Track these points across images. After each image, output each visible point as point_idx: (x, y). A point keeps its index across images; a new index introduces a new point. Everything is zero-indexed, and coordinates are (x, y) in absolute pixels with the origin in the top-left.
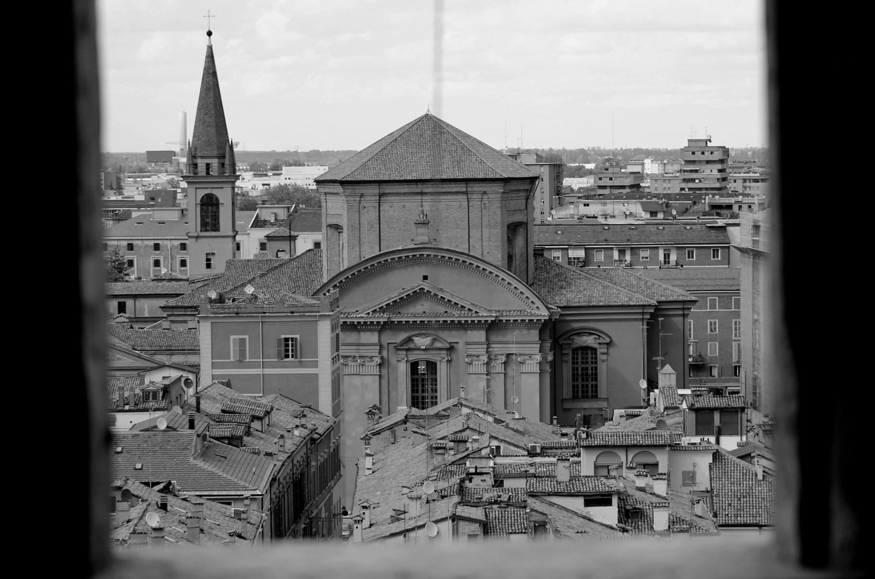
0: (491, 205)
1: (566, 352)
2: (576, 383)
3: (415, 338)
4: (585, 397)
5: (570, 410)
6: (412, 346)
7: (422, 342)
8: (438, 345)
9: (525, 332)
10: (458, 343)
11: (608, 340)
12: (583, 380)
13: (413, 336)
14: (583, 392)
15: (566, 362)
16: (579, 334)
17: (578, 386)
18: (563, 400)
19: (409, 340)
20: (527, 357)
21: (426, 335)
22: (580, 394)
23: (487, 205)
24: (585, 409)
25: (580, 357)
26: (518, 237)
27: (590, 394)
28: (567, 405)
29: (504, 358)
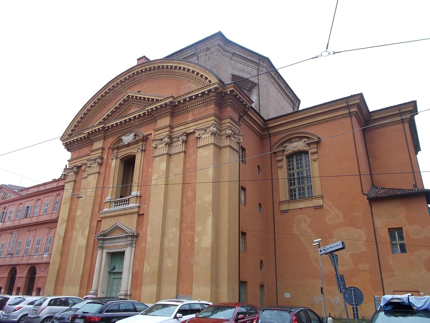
1: (280, 158)
2: (293, 187)
3: (123, 138)
4: (303, 198)
5: (287, 211)
6: (121, 144)
7: (127, 139)
8: (137, 138)
9: (203, 109)
11: (316, 139)
12: (299, 183)
14: (300, 194)
15: (281, 168)
16: (289, 141)
17: (295, 189)
18: (281, 203)
21: (130, 132)
22: (297, 197)
23: (210, 57)
24: (301, 208)
25: (295, 163)
26: (253, 96)
27: (307, 196)
28: (284, 207)
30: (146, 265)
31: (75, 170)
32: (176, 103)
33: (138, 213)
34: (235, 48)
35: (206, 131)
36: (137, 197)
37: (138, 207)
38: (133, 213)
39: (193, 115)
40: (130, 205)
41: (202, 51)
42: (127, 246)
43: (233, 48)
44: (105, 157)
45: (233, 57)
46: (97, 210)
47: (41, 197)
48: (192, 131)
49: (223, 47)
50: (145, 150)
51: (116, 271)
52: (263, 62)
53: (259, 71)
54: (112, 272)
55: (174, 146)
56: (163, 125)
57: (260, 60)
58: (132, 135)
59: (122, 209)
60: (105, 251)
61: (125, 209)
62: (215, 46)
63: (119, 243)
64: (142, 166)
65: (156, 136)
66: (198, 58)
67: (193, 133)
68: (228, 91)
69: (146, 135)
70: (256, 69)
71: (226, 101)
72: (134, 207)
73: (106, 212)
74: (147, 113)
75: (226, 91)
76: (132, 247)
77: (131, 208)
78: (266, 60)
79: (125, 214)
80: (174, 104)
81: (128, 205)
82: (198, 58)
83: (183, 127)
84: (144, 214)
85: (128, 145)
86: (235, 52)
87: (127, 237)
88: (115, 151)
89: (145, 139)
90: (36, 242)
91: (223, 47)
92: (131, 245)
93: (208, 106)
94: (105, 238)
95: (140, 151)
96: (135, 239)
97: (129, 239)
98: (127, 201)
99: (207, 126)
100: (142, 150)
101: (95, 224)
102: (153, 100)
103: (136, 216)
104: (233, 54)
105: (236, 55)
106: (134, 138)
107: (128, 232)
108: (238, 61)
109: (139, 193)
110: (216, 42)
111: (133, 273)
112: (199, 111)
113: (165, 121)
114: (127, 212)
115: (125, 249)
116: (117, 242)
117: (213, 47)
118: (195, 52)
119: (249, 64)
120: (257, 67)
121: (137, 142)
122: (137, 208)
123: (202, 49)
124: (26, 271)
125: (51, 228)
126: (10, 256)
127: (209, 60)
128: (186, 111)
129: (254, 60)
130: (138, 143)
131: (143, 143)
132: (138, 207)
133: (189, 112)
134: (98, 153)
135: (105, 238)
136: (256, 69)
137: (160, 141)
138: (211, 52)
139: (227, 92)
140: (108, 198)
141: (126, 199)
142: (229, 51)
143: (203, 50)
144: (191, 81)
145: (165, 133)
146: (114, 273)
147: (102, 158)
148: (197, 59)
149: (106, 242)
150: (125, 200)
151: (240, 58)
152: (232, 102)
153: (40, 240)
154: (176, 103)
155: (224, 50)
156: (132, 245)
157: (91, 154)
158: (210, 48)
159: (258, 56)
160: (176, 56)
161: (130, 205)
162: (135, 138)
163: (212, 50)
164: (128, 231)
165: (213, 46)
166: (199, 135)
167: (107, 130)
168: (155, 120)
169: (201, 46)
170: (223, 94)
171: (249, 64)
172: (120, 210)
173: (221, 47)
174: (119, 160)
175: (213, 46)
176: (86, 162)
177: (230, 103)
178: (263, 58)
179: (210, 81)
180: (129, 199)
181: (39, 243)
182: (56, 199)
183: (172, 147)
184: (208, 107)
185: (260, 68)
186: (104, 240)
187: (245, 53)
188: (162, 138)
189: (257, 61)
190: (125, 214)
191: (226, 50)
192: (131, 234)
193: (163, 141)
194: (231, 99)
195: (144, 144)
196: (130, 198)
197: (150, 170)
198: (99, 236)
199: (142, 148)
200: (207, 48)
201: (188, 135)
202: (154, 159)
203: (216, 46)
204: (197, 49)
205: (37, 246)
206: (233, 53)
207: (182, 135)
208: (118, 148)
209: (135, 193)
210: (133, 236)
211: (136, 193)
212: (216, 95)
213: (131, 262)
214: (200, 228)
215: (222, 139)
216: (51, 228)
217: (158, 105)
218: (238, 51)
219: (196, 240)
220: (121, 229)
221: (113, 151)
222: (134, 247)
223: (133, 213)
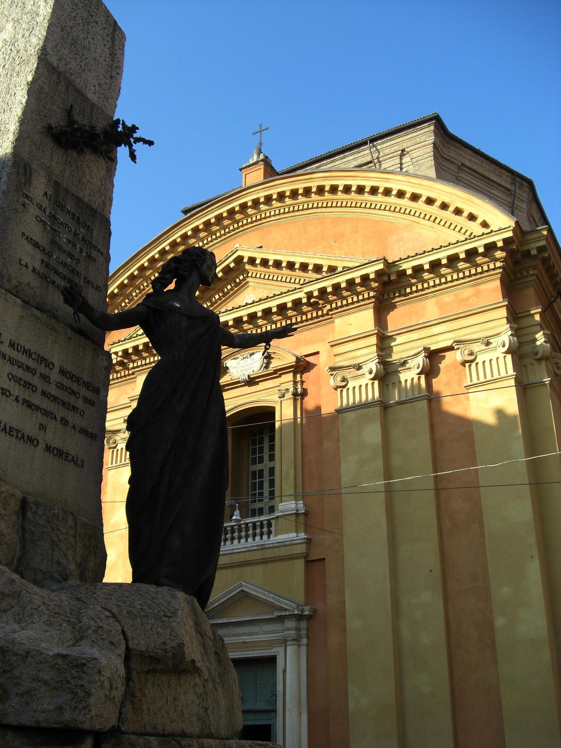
0: (417, 167)
8: (275, 364)
10: (317, 353)
20: (477, 347)
29: (420, 360)
30: (353, 692)
32: (393, 277)
33: (306, 558)
34: (463, 154)
36: (297, 514)
37: (306, 543)
38: (292, 557)
39: (441, 306)
40: (275, 539)
41: (390, 158)
42: (284, 642)
43: (460, 152)
45: (461, 175)
48: (449, 343)
49: (440, 151)
52: (520, 188)
53: (514, 209)
55: (394, 383)
56: (353, 331)
57: (513, 183)
59: (255, 548)
61: (263, 548)
62: (423, 147)
63: (253, 637)
64: (299, 436)
65: (338, 359)
67: (450, 348)
68: (533, 249)
70: (506, 203)
71: (525, 274)
72: (295, 542)
74: (304, 301)
75: (526, 248)
76: (299, 646)
77: (282, 545)
78: (530, 183)
79: (265, 561)
80: (386, 278)
81: (269, 537)
83: (414, 335)
84: (324, 559)
85: (251, 381)
86: (464, 162)
87: (281, 619)
91: (440, 151)
92: (297, 640)
93: (481, 284)
95: (289, 395)
96: (304, 624)
97: (290, 624)
99: (490, 334)
100: (295, 394)
103: (300, 564)
104: (460, 168)
105: (465, 169)
106: (264, 365)
107: (287, 607)
108: (471, 184)
110: (426, 138)
111: (309, 712)
112: (456, 295)
114: (268, 554)
116: (245, 634)
117: (419, 148)
118: (369, 159)
119: (494, 192)
120: (510, 200)
121: (278, 373)
122: (302, 543)
123: (387, 152)
128: (422, 294)
129: (503, 183)
130: (280, 376)
131: (295, 377)
132: (306, 543)
133: (427, 299)
136: (506, 203)
137: (353, 370)
138: (414, 160)
139: (529, 251)
141: (262, 522)
143: (391, 155)
144: (418, 223)
150: (259, 523)
151: (474, 176)
152: (537, 276)
154: (393, 277)
155: (443, 157)
156: (299, 641)
158: (411, 151)
159: (509, 174)
161: (275, 539)
162: (268, 364)
163: (415, 155)
164: (286, 604)
165: (419, 145)
168: (330, 316)
169: (385, 145)
170: (519, 256)
171: (494, 192)
172: (249, 551)
175: (417, 146)
177: (534, 278)
178: (520, 180)
179: (485, 225)
180: (269, 521)
183: (388, 385)
184: (482, 287)
185: (516, 202)
187: (484, 165)
188: (358, 364)
189: (508, 186)
190: (265, 561)
192: (296, 612)
193: (365, 369)
194: (536, 269)
196: (273, 519)
197: (327, 444)
199: (296, 389)
200: (403, 150)
202: (340, 415)
206: (460, 164)
210: (300, 618)
211: (294, 506)
212: (505, 258)
213: (300, 684)
214: (506, 590)
215: (525, 366)
217: (342, 279)
218: (470, 160)
219: (499, 621)
220: (257, 600)
222: (303, 645)
223: (292, 557)
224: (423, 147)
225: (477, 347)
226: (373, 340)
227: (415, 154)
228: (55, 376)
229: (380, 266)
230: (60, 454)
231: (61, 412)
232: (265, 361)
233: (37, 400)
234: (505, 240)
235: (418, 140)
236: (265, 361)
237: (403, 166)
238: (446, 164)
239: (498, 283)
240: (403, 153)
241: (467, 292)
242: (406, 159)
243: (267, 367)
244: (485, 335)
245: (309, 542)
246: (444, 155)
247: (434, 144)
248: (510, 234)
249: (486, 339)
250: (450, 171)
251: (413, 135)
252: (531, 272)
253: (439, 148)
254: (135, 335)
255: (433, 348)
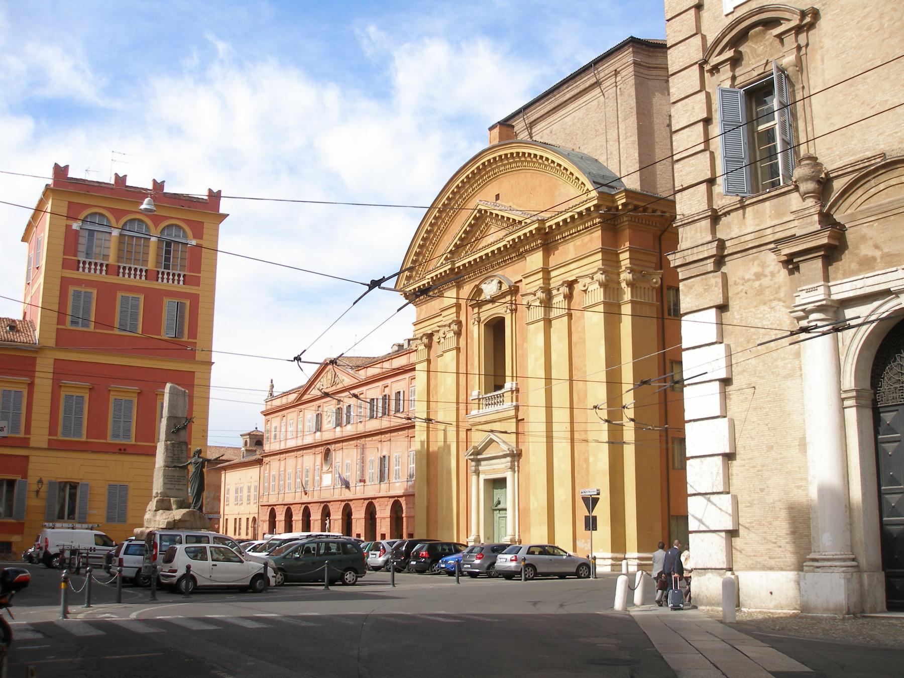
3: (483, 286)
7: (490, 289)
13: (480, 283)
19: (479, 291)
30: (532, 499)
31: (425, 340)
35: (593, 279)
36: (512, 391)
39: (576, 248)
44: (463, 318)
46: (462, 412)
47: (388, 382)
50: (516, 310)
51: (500, 507)
54: (496, 508)
58: (495, 282)
60: (482, 477)
66: (602, 91)
69: (516, 283)
73: (475, 417)
75: (615, 205)
77: (505, 411)
80: (543, 231)
82: (602, 91)
83: (562, 270)
84: (523, 419)
85: (493, 300)
88: (476, 310)
89: (514, 290)
90: (395, 460)
91: (645, 64)
94: (479, 457)
97: (509, 459)
98: (500, 400)
99: (593, 272)
100: (511, 310)
101: (463, 435)
102: (514, 220)
106: (499, 288)
109: (514, 385)
112: (582, 240)
113: (535, 260)
115: (506, 473)
121: (503, 295)
123: (607, 72)
124: (389, 508)
125: (411, 437)
126: (362, 484)
127: (621, 94)
131: (512, 297)
134: (451, 315)
135: (479, 457)
138: (623, 79)
139: (617, 207)
140: (475, 393)
142: (661, 66)
143: (609, 75)
145: (537, 282)
146: (500, 510)
147: (459, 323)
148: (601, 94)
149: (483, 463)
153: (399, 458)
157: (444, 314)
160: (567, 88)
161: (505, 406)
162: (501, 287)
166: (585, 286)
167: (458, 273)
173: (640, 65)
174: (482, 326)
176: (438, 329)
180: (503, 394)
181: (399, 462)
182: (410, 386)
186: (478, 462)
191: (652, 65)
192: (508, 452)
195: (514, 298)
197: (525, 344)
198: (470, 455)
200: (616, 70)
201: (571, 285)
202: (528, 326)
203: (629, 66)
204: (599, 73)
205: (397, 468)
207: (562, 285)
208: (480, 305)
209: (508, 385)
216: (411, 437)
219: (591, 459)
221: (473, 309)
224: (627, 66)
225: (588, 280)
226: (540, 275)
227: (624, 73)
228: (176, 478)
229: (536, 225)
230: (178, 489)
231: (177, 483)
232: (499, 285)
233: (173, 482)
234: (594, 206)
235: (624, 61)
236: (499, 285)
237: (618, 84)
238: (655, 72)
239: (600, 232)
240: (616, 73)
241: (586, 238)
242: (618, 78)
243: (500, 289)
244: (591, 273)
245: (517, 408)
246: (650, 65)
247: (635, 63)
248: (595, 202)
249: (591, 276)
250: (659, 78)
251: (620, 56)
252: (625, 219)
253: (642, 63)
254: (438, 265)
255: (570, 279)
